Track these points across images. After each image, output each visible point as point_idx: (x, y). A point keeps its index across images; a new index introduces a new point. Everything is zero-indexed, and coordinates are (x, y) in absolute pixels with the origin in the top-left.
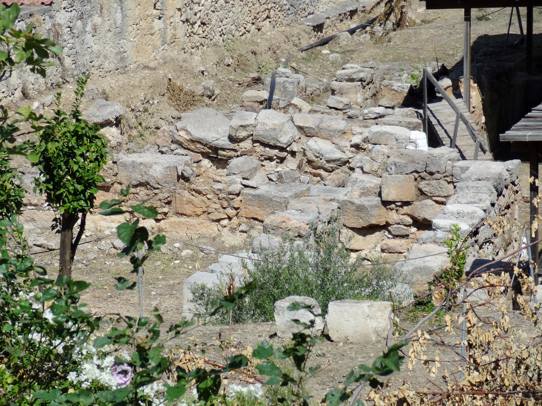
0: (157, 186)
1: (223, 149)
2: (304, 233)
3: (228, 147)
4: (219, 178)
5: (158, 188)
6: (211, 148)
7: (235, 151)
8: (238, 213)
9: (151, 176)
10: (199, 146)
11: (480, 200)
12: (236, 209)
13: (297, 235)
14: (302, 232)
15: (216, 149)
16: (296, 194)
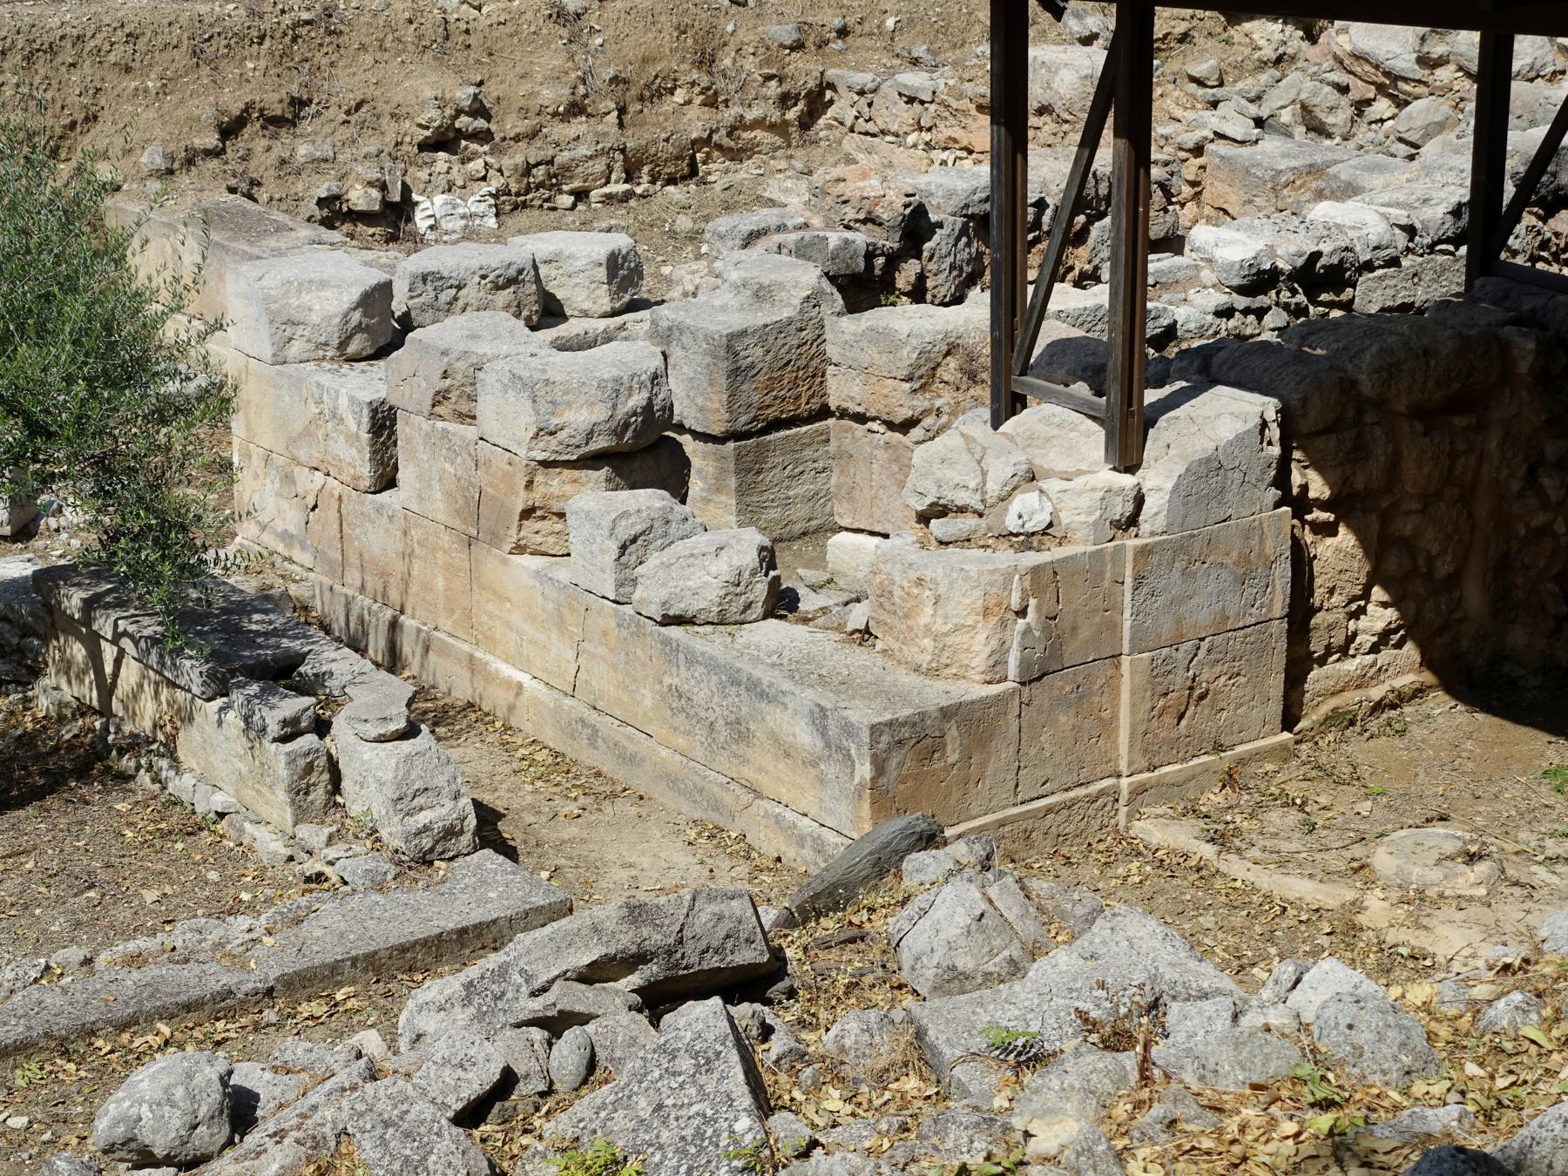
0: (1066, 116)
1: (1406, 80)
2: (885, 216)
3: (1411, 76)
4: (1178, 113)
5: (1067, 122)
6: (1387, 74)
7: (1425, 84)
8: (1200, 193)
9: (1057, 93)
10: (1367, 68)
11: (1425, 201)
12: (1193, 184)
13: (862, 216)
14: (879, 211)
15: (1396, 78)
16: (1311, 166)
